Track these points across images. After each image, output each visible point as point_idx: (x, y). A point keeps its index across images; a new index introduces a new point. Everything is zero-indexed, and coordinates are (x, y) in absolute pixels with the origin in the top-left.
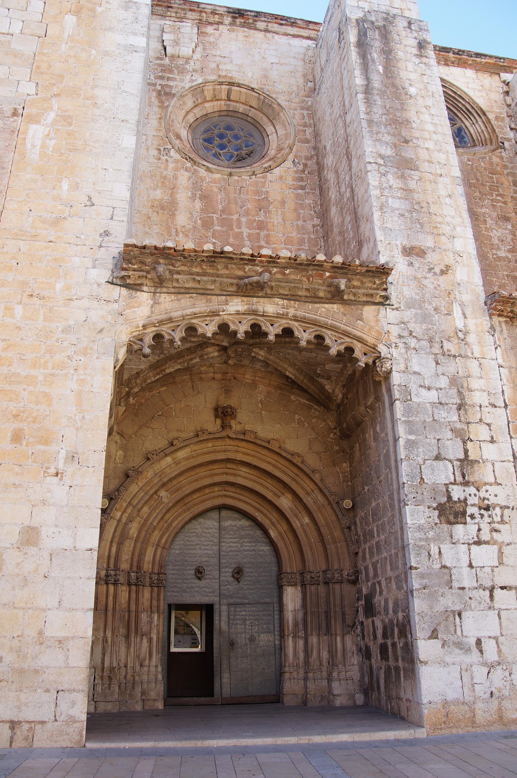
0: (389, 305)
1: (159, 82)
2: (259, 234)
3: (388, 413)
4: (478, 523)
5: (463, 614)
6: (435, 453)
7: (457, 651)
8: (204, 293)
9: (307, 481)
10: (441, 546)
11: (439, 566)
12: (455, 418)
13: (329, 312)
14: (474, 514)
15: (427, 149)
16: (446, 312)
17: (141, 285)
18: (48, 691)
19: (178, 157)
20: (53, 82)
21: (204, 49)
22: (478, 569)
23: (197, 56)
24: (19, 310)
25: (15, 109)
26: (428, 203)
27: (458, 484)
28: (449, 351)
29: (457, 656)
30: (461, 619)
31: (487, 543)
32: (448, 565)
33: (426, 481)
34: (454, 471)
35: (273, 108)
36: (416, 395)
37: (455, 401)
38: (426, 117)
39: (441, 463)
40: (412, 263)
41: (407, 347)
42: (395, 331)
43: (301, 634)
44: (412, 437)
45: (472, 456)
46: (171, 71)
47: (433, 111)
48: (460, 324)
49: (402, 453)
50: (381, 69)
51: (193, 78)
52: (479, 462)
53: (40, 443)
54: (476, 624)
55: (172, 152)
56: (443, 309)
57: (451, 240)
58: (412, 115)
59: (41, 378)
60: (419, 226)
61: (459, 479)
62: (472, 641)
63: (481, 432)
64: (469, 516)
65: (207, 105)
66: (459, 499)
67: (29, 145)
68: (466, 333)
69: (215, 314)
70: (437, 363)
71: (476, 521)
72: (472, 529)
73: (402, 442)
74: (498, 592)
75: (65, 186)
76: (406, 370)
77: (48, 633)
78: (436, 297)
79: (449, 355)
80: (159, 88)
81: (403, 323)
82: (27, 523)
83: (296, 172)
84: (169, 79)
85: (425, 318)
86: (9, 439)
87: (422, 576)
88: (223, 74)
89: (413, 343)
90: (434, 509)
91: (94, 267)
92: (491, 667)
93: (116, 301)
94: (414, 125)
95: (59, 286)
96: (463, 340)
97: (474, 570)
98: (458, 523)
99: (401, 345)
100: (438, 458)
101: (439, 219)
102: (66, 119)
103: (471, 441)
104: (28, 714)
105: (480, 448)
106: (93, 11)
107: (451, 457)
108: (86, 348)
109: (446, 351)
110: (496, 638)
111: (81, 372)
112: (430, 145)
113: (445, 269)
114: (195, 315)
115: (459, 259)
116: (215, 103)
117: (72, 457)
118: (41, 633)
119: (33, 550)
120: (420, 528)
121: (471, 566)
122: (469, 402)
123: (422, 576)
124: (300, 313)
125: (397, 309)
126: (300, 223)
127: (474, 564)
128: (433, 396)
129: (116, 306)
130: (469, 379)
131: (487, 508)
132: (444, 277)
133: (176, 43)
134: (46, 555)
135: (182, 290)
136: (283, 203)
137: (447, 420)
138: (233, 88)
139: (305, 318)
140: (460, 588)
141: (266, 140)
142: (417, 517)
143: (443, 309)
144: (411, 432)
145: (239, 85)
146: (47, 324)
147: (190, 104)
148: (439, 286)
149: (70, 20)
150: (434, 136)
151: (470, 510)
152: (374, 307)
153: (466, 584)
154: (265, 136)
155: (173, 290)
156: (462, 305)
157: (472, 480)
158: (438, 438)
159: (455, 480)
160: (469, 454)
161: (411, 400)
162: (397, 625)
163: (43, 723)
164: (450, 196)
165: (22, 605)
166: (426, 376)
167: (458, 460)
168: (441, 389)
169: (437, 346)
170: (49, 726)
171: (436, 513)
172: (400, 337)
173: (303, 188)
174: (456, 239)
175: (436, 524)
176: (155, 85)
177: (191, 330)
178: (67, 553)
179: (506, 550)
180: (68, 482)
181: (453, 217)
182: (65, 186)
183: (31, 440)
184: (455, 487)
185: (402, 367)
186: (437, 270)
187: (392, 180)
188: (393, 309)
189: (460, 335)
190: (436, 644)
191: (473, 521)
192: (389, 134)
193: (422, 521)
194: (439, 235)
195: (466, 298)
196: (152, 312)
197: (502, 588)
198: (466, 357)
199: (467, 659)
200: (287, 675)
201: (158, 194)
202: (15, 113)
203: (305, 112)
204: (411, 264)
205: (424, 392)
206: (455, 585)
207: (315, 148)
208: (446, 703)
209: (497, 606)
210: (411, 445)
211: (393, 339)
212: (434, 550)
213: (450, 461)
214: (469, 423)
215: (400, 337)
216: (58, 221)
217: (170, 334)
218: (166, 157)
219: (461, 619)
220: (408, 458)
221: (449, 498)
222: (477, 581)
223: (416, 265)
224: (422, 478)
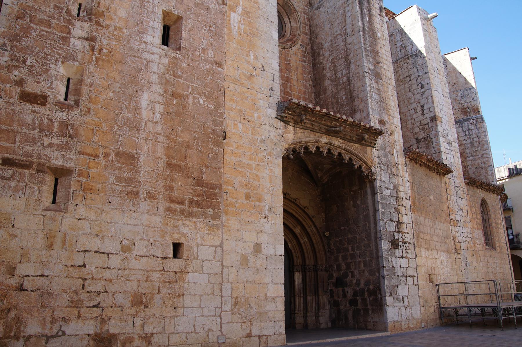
2: (287, 84)
3: (369, 197)
7: (397, 301)
8: (313, 130)
9: (309, 221)
12: (395, 203)
13: (355, 147)
17: (289, 122)
18: (271, 321)
24: (240, 126)
29: (397, 304)
31: (405, 257)
35: (291, 9)
38: (384, 51)
43: (302, 295)
44: (383, 210)
53: (257, 201)
54: (402, 291)
58: (379, 48)
59: (254, 166)
61: (397, 230)
62: (401, 297)
63: (403, 210)
67: (232, 26)
68: (398, 165)
69: (316, 142)
74: (408, 278)
77: (269, 295)
82: (256, 242)
83: (302, 51)
85: (386, 156)
86: (244, 197)
87: (387, 270)
91: (269, 108)
92: (406, 307)
93: (280, 129)
94: (380, 55)
95: (256, 115)
101: (389, 107)
102: (246, 13)
104: (265, 332)
107: (394, 220)
108: (270, 152)
110: (407, 296)
111: (270, 165)
112: (385, 67)
114: (310, 142)
117: (270, 209)
118: (266, 295)
119: (259, 255)
120: (386, 250)
121: (400, 267)
123: (387, 270)
124: (347, 147)
125: (377, 150)
126: (304, 82)
129: (280, 131)
131: (405, 244)
134: (264, 257)
135: (305, 128)
136: (297, 68)
139: (348, 149)
141: (284, 25)
142: (385, 245)
144: (383, 208)
146: (253, 136)
152: (370, 148)
154: (283, 23)
155: (301, 127)
156: (397, 151)
162: (367, 291)
163: (270, 336)
165: (258, 282)
169: (390, 169)
170: (273, 336)
173: (305, 61)
177: (306, 148)
178: (273, 257)
179: (410, 261)
180: (270, 222)
183: (253, 199)
190: (391, 298)
196: (294, 137)
197: (409, 276)
198: (398, 176)
200: (296, 315)
203: (305, 16)
206: (396, 274)
207: (310, 39)
208: (394, 321)
209: (408, 283)
210: (383, 213)
215: (379, 163)
216: (251, 77)
217: (299, 150)
221: (394, 238)
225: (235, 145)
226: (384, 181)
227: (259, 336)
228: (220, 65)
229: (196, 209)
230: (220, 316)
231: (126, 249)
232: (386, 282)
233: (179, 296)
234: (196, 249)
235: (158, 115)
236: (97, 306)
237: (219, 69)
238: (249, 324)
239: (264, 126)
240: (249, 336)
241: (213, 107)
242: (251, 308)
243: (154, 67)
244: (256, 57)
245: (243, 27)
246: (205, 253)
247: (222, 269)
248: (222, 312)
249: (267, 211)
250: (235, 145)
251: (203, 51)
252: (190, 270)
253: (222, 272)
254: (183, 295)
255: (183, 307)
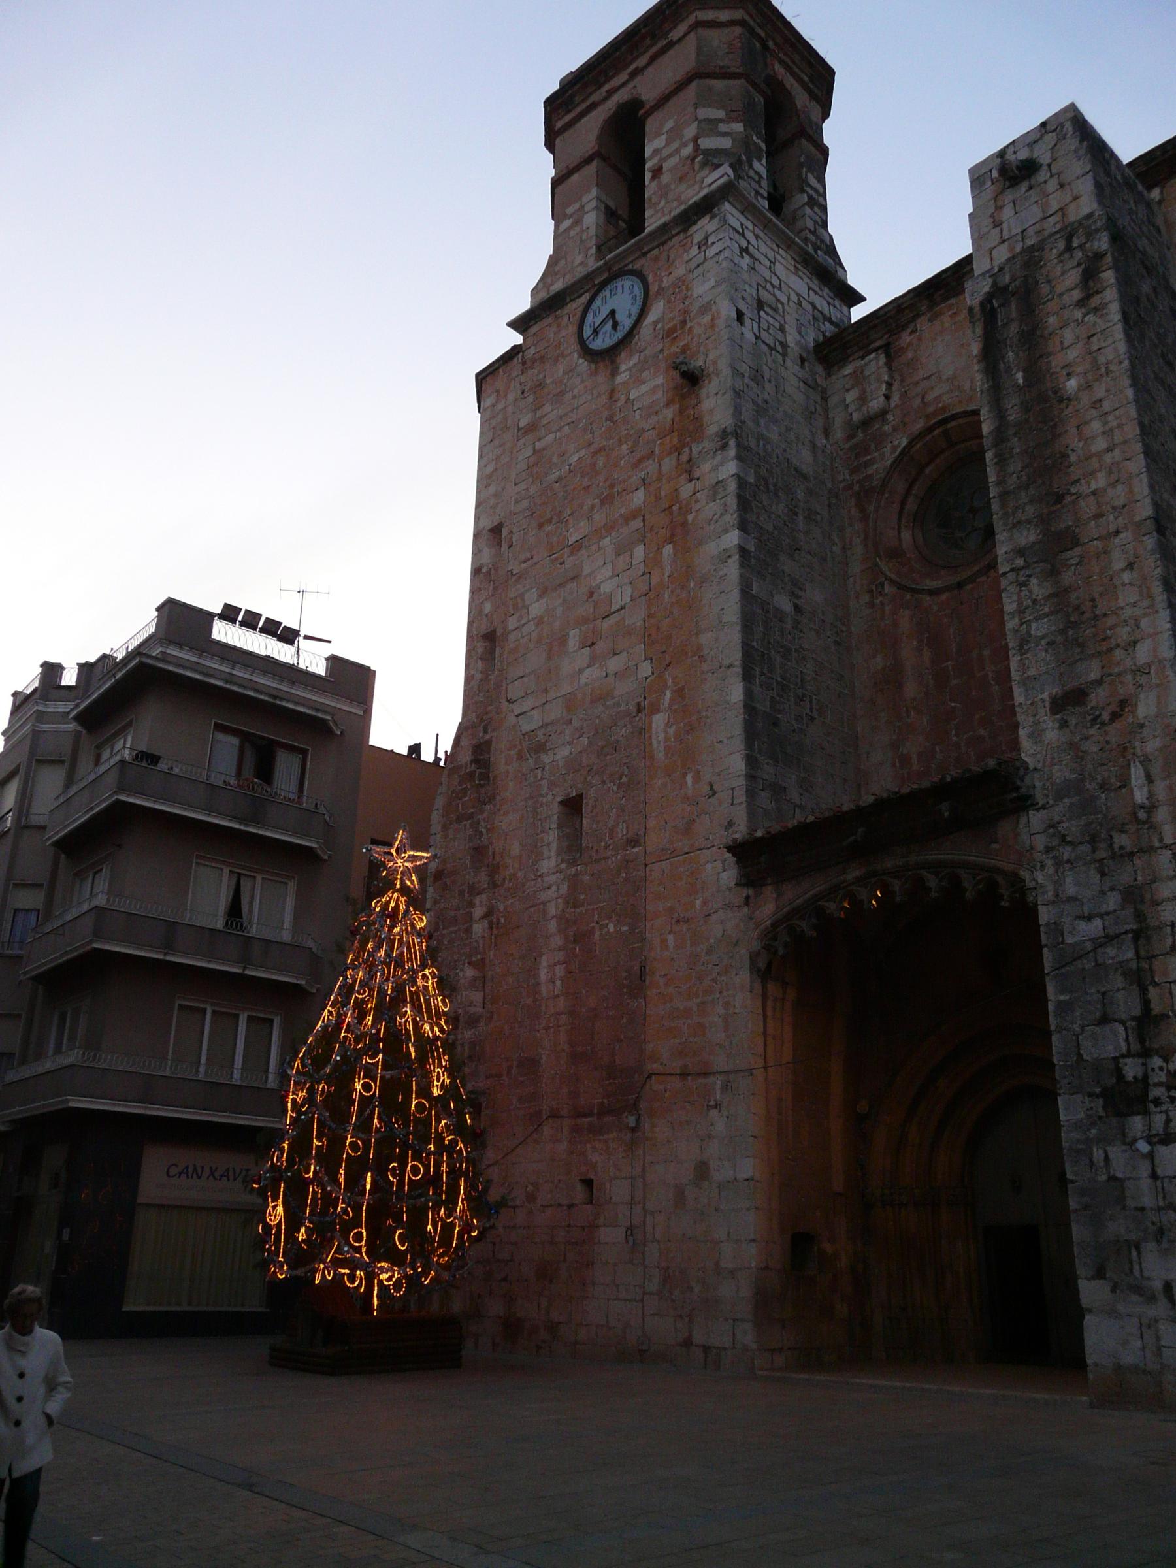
0: (1032, 805)
1: (856, 478)
4: (1166, 1112)
5: (1143, 1245)
6: (1098, 1014)
7: (1135, 1298)
10: (1109, 1149)
11: (1104, 1177)
12: (1130, 954)
14: (1159, 1098)
15: (1094, 493)
16: (1118, 784)
18: (727, 1320)
19: (894, 589)
20: (664, 648)
21: (902, 381)
22: (1166, 1180)
23: (896, 399)
25: (638, 703)
26: (1093, 600)
27: (1133, 1056)
28: (1121, 848)
30: (1139, 1254)
32: (1119, 1175)
33: (1085, 1057)
34: (1127, 1036)
36: (1071, 932)
37: (1128, 927)
39: (1107, 1028)
40: (1066, 722)
41: (1058, 863)
42: (1040, 842)
45: (1156, 1008)
46: (867, 451)
47: (1106, 406)
48: (1140, 796)
49: (1053, 1023)
50: (1020, 377)
51: (896, 443)
52: (1168, 1017)
55: (887, 589)
56: (1113, 780)
57: (1130, 651)
58: (1071, 439)
59: (695, 1009)
60: (1077, 650)
61: (1135, 1047)
62: (1158, 1285)
64: (1152, 1101)
65: (927, 471)
66: (1135, 1078)
68: (1151, 808)
70: (1103, 874)
71: (1164, 1108)
72: (1158, 1120)
73: (1051, 1007)
75: (689, 779)
76: (1057, 899)
77: (723, 1265)
78: (1103, 765)
79: (1122, 856)
80: (857, 488)
81: (1053, 826)
84: (867, 464)
88: (931, 409)
89: (1067, 853)
90: (1098, 1097)
96: (1144, 823)
97: (1159, 1183)
98: (1133, 1114)
99: (1049, 862)
100: (1104, 1020)
102: (679, 692)
103: (1157, 984)
105: (1171, 993)
106: (684, 524)
107: (1124, 1016)
109: (1116, 850)
111: (725, 994)
112: (1100, 482)
113: (1118, 709)
115: (1143, 680)
116: (938, 461)
118: (717, 1264)
121: (1154, 1176)
122: (1153, 923)
125: (1044, 808)
127: (1159, 1172)
128: (1095, 927)
130: (1154, 886)
132: (1117, 725)
133: (863, 399)
137: (1119, 959)
138: (949, 426)
140: (1137, 1209)
143: (1113, 780)
145: (953, 417)
147: (900, 486)
148: (1108, 742)
149: (668, 550)
150: (1108, 458)
151: (1155, 1092)
153: (1147, 1201)
156: (1146, 761)
157: (1156, 1046)
158: (1103, 990)
159: (1129, 1050)
160: (1152, 1006)
161: (1063, 943)
163: (725, 1349)
164: (1130, 566)
166: (1085, 900)
167: (1134, 1018)
168: (1108, 914)
171: (1101, 1101)
172: (1048, 850)
174: (1139, 646)
175: (1100, 1118)
176: (850, 487)
181: (1134, 605)
182: (689, 779)
184: (1129, 1060)
185: (1050, 895)
186: (1106, 716)
187: (1038, 588)
188: (1038, 810)
189: (1142, 815)
191: (1158, 1109)
192: (1031, 502)
193: (1082, 1115)
194: (1111, 650)
195: (1152, 745)
199: (1151, 1312)
201: (879, 662)
202: (639, 711)
204: (1064, 724)
205: (1082, 925)
206: (1130, 1203)
208: (1118, 1368)
211: (1038, 856)
212: (1098, 1154)
213: (1122, 1022)
214: (1154, 956)
216: (688, 829)
218: (881, 599)
219: (1139, 1254)
220: (1060, 1029)
222: (1164, 1197)
223: (1073, 721)
224: (1080, 1055)
225: (662, 981)
226: (1072, 899)
227: (704, 1346)
228: (634, 842)
229: (608, 1119)
230: (642, 1301)
231: (531, 1198)
232: (1078, 1232)
233: (588, 1265)
234: (608, 1186)
235: (558, 983)
236: (505, 1279)
237: (636, 850)
238: (687, 1320)
239: (714, 917)
240: (688, 1343)
241: (625, 928)
242: (690, 1289)
243: (552, 910)
244: (697, 779)
245: (672, 731)
246: (619, 1191)
247: (645, 1217)
248: (644, 1294)
249: (718, 1092)
250: (662, 981)
251: (612, 832)
252: (601, 1221)
253: (644, 1222)
254: (593, 1263)
255: (594, 1284)
